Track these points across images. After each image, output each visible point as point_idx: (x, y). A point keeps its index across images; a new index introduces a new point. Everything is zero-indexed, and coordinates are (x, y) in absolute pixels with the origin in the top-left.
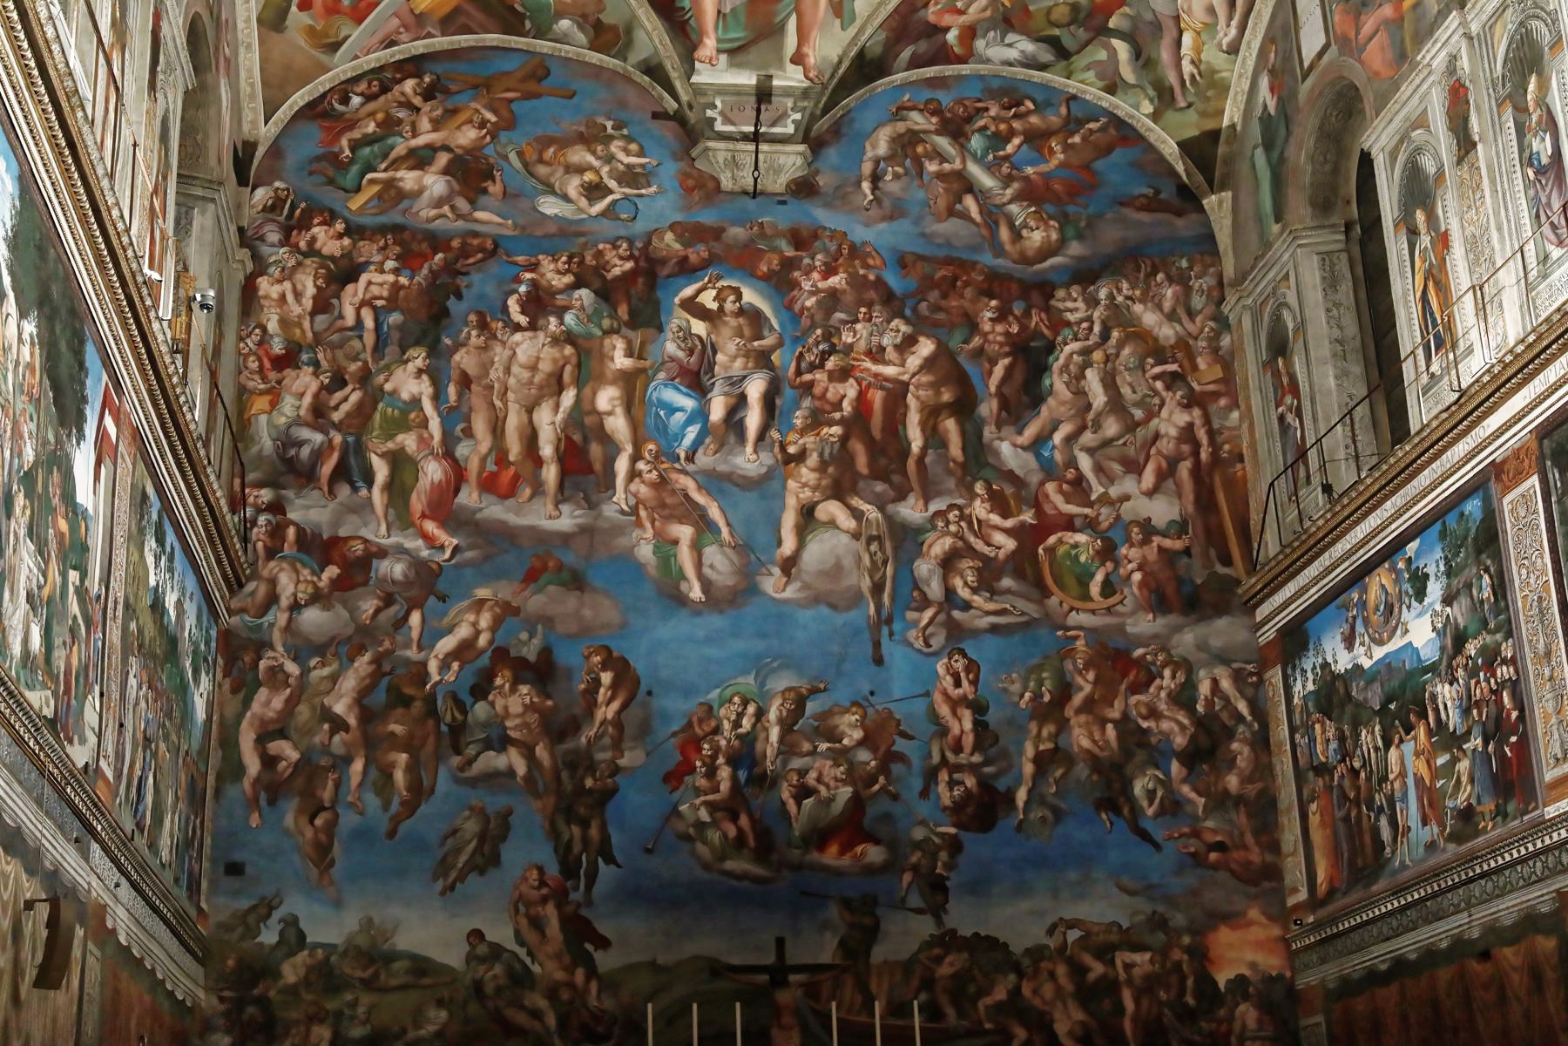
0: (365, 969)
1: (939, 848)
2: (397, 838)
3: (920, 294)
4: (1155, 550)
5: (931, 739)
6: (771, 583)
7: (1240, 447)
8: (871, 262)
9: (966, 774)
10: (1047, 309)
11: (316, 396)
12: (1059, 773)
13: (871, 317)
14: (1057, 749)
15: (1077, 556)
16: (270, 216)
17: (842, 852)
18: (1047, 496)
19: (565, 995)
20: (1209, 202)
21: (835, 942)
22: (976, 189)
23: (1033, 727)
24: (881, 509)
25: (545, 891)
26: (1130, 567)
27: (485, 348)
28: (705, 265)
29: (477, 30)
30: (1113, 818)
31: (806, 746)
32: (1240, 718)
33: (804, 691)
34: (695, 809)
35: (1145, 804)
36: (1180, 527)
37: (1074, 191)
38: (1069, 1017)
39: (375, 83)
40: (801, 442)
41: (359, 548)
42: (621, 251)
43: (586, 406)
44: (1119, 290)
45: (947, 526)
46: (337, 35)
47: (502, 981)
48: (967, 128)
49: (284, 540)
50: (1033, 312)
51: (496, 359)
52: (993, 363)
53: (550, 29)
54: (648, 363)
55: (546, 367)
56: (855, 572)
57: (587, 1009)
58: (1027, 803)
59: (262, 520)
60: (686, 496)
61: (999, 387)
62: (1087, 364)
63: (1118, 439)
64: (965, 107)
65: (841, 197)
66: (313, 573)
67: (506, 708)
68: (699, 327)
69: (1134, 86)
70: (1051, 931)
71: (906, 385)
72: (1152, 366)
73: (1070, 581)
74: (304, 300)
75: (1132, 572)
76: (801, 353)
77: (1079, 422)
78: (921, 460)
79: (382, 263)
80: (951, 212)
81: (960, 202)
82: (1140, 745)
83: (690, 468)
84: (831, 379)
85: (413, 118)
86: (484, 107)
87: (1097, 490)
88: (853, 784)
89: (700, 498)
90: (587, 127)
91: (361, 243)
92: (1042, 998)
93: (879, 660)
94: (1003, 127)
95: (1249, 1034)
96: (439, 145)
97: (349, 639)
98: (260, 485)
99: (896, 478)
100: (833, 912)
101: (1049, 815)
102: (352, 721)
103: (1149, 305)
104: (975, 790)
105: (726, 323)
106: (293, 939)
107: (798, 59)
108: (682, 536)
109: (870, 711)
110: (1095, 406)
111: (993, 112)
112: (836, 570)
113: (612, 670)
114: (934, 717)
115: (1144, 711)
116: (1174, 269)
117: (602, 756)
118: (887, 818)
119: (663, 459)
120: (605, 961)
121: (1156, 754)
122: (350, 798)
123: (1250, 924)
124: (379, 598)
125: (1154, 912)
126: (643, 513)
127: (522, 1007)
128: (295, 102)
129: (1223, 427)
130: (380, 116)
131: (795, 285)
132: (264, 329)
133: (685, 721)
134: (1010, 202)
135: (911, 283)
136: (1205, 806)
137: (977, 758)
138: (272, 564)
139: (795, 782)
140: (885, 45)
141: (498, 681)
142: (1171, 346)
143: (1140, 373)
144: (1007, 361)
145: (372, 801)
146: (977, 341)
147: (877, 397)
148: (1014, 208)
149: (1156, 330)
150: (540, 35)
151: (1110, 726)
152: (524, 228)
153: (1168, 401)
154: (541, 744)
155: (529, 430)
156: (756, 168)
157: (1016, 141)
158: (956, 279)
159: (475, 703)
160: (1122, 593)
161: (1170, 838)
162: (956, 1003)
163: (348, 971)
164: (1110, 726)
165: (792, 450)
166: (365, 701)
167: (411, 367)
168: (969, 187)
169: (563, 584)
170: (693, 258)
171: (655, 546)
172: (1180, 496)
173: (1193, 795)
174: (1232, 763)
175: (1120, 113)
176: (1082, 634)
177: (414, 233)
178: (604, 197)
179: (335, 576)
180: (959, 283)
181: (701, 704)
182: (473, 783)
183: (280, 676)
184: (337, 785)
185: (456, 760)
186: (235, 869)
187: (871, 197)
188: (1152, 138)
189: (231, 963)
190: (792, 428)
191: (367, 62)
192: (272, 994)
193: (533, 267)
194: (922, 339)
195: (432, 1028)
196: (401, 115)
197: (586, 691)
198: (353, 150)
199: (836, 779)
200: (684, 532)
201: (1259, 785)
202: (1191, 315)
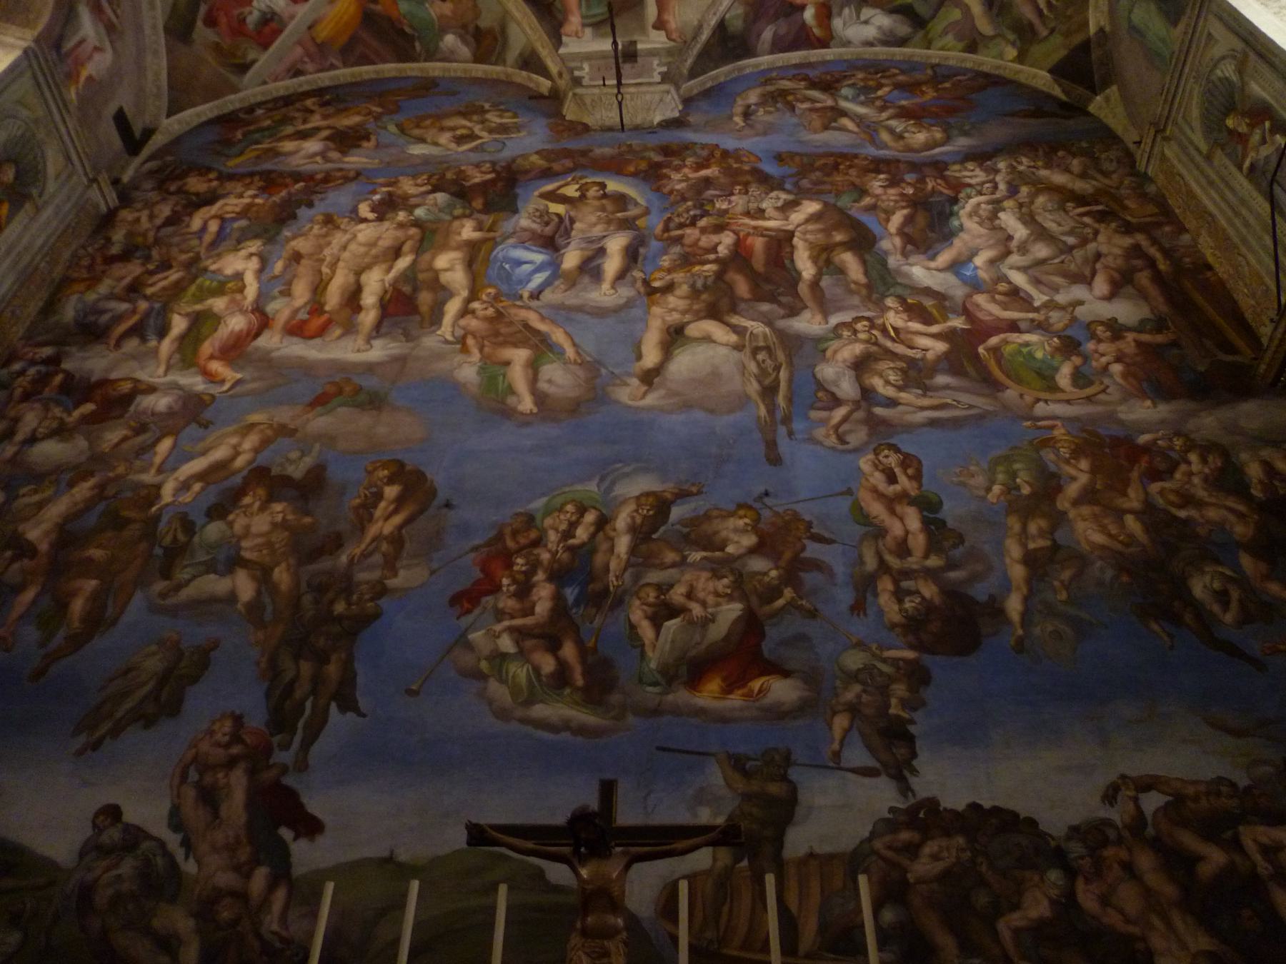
1: (891, 679)
4: (1133, 344)
6: (628, 393)
12: (1066, 575)
14: (1056, 547)
17: (728, 690)
18: (978, 306)
20: (1096, 105)
24: (769, 323)
26: (1104, 360)
28: (570, 170)
33: (668, 496)
35: (1216, 608)
37: (952, 111)
40: (668, 277)
41: (126, 387)
42: (483, 169)
43: (423, 265)
44: (1020, 163)
50: (928, 180)
52: (889, 213)
53: (437, 47)
55: (385, 243)
57: (259, 936)
58: (1025, 615)
64: (832, 76)
67: (247, 527)
69: (992, 38)
70: (1110, 796)
71: (791, 235)
75: (1108, 364)
77: (1002, 248)
78: (815, 285)
83: (534, 303)
87: (1039, 298)
88: (744, 597)
89: (543, 327)
92: (1121, 911)
93: (775, 459)
104: (937, 600)
105: (587, 204)
107: (660, 25)
109: (766, 513)
114: (862, 516)
117: (362, 576)
118: (800, 639)
119: (502, 299)
126: (470, 341)
130: (276, 118)
133: (492, 533)
134: (888, 119)
137: (934, 561)
139: (651, 599)
140: (745, 21)
141: (247, 500)
147: (758, 244)
148: (893, 123)
150: (431, 55)
154: (284, 565)
158: (839, 164)
159: (208, 523)
160: (1102, 383)
165: (656, 284)
167: (243, 253)
168: (844, 113)
169: (357, 406)
176: (1058, 423)
177: (281, 174)
181: (517, 514)
182: (174, 612)
185: (160, 586)
190: (660, 269)
197: (363, 506)
199: (717, 594)
200: (520, 355)
202: (1106, 174)
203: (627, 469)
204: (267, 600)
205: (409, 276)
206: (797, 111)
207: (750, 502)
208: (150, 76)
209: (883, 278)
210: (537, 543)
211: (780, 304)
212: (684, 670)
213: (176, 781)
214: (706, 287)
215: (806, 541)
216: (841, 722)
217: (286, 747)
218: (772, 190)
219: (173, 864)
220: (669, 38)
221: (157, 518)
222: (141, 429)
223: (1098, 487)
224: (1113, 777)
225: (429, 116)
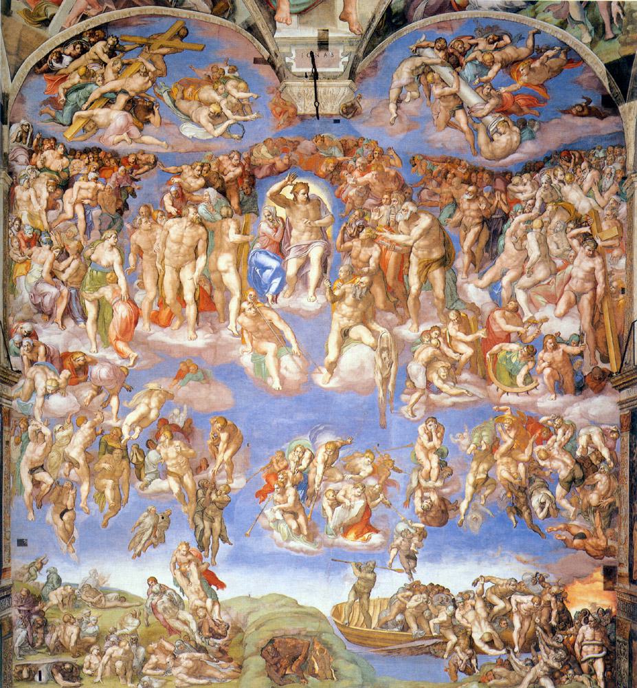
2: (108, 527)
3: (424, 183)
4: (561, 354)
8: (392, 162)
9: (432, 493)
10: (506, 191)
11: (52, 264)
12: (487, 492)
13: (390, 202)
14: (487, 477)
15: (510, 358)
16: (20, 144)
17: (357, 537)
18: (495, 320)
19: (201, 613)
22: (465, 106)
23: (474, 465)
24: (390, 330)
25: (190, 557)
26: (544, 365)
27: (150, 230)
29: (139, 4)
31: (339, 477)
32: (603, 460)
33: (338, 444)
35: (538, 510)
36: (579, 338)
38: (482, 630)
40: (342, 287)
41: (80, 360)
42: (233, 161)
43: (212, 267)
44: (555, 176)
47: (167, 605)
48: (462, 60)
51: (158, 237)
52: (467, 229)
54: (249, 238)
55: (187, 241)
56: (372, 369)
58: (467, 510)
59: (25, 342)
61: (470, 248)
63: (544, 280)
67: (167, 454)
68: (282, 212)
70: (475, 584)
72: (572, 229)
73: (505, 375)
74: (42, 201)
78: (417, 297)
80: (448, 124)
81: (454, 116)
83: (275, 306)
84: (362, 245)
85: (102, 71)
86: (146, 60)
87: (527, 315)
89: (280, 325)
91: (74, 161)
93: (384, 427)
94: (487, 57)
95: (585, 642)
96: (119, 89)
98: (24, 321)
100: (351, 570)
102: (81, 461)
105: (298, 209)
112: (362, 368)
115: (543, 455)
116: (594, 159)
117: (221, 482)
120: (222, 595)
122: (81, 505)
125: (537, 573)
126: (246, 336)
127: (178, 619)
130: (82, 70)
131: (341, 181)
137: (439, 484)
138: (32, 369)
139: (331, 497)
141: (162, 438)
143: (563, 234)
144: (477, 229)
146: (458, 216)
147: (392, 257)
148: (490, 119)
149: (576, 206)
153: (579, 254)
155: (178, 283)
157: (496, 68)
159: (149, 451)
162: (416, 619)
163: (84, 598)
165: (337, 293)
167: (107, 244)
169: (198, 380)
170: (279, 165)
173: (568, 506)
174: (594, 486)
175: (568, 42)
178: (223, 122)
180: (449, 176)
183: (40, 435)
185: (139, 484)
187: (395, 115)
192: (45, 609)
193: (179, 174)
194: (422, 216)
196: (95, 69)
197: (213, 444)
198: (66, 96)
199: (355, 496)
200: (270, 347)
201: (610, 500)
202: (601, 191)
203: (321, 428)
205: (205, 277)
210: (286, 467)
211: (397, 314)
216: (394, 552)
218: (405, 201)
222: (99, 390)
225: (189, 83)
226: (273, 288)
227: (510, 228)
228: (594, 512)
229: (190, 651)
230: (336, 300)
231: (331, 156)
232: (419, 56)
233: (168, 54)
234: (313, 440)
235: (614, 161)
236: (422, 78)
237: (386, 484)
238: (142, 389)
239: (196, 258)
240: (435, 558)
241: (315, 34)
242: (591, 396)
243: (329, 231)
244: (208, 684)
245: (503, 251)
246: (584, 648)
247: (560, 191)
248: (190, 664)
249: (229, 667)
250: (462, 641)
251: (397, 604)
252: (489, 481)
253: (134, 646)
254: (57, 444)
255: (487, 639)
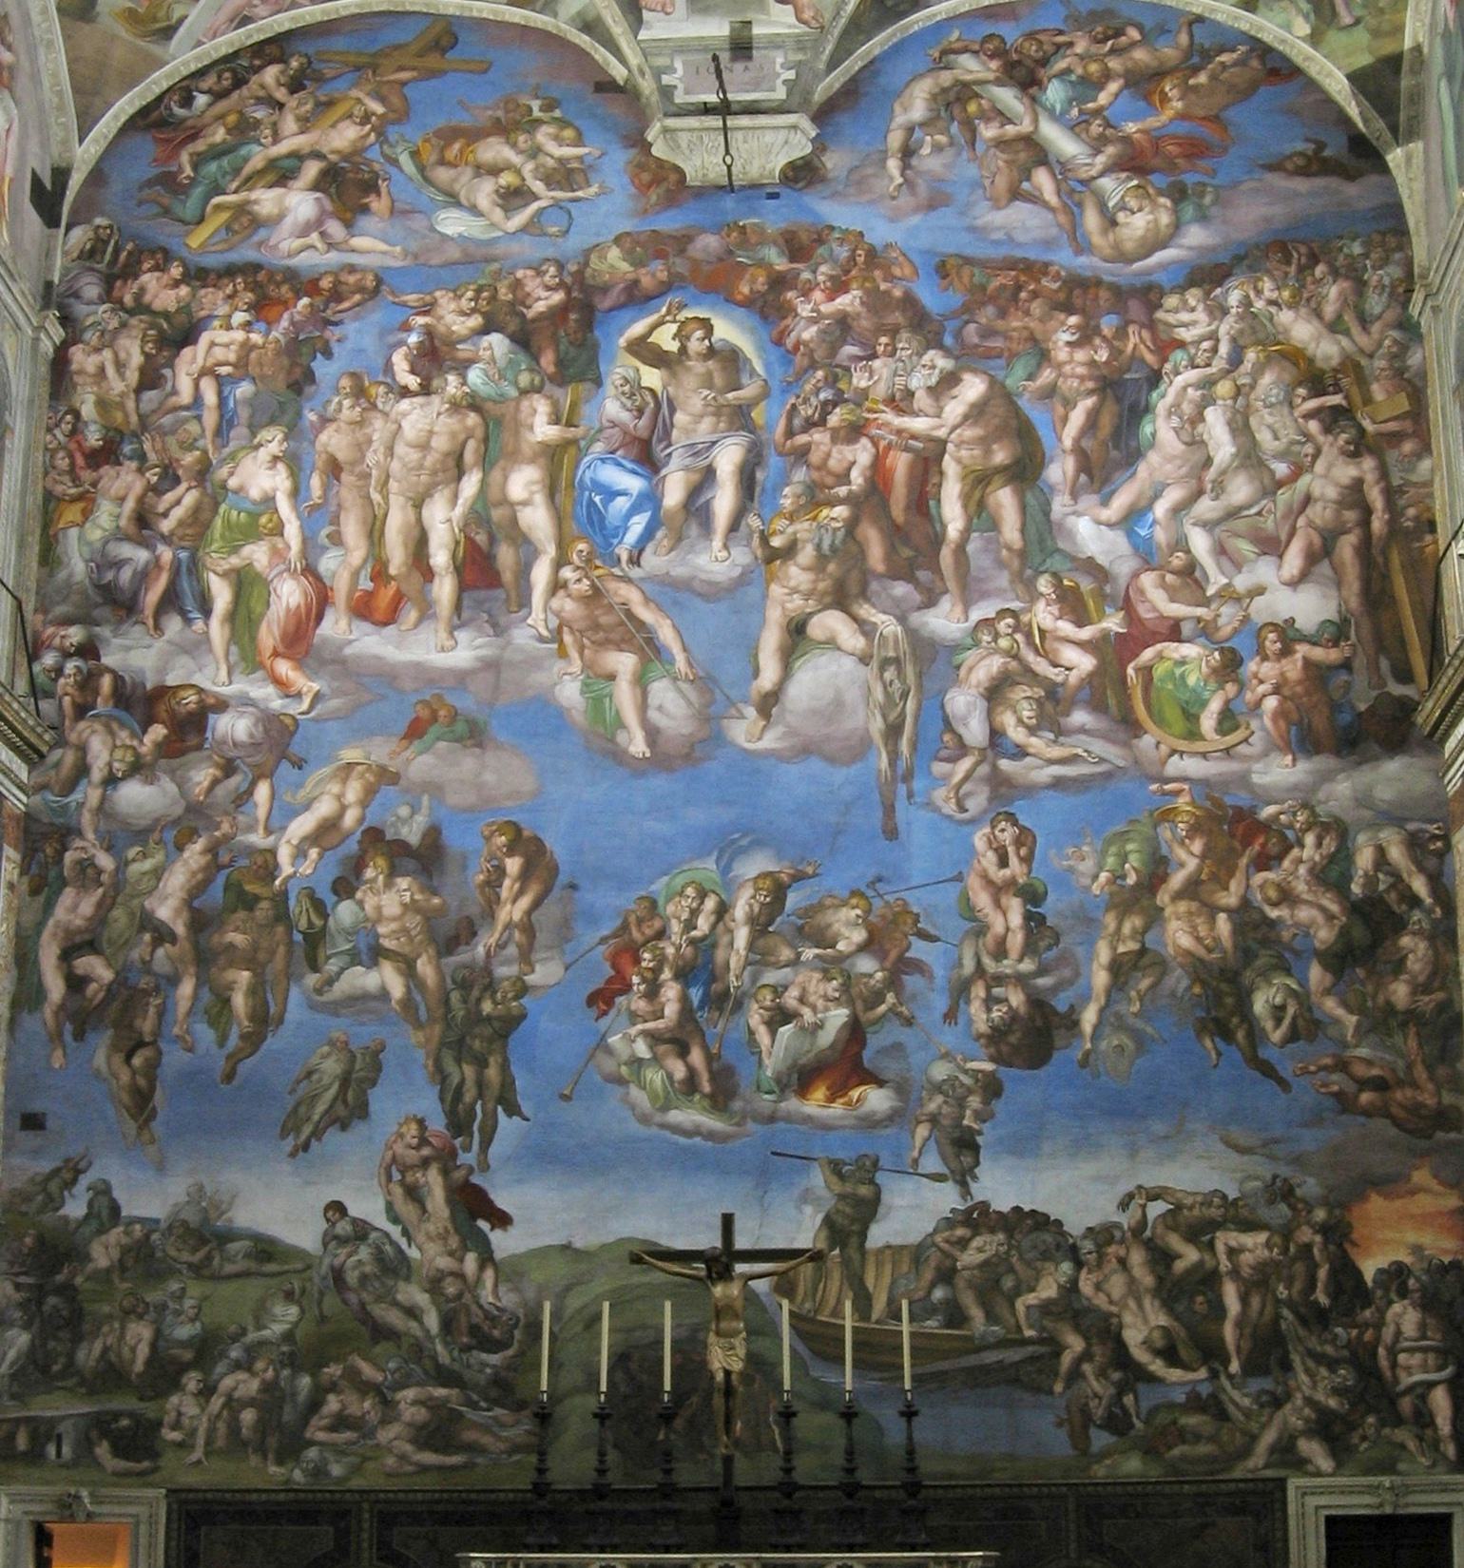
0: (194, 1250)
3: (968, 310)
4: (1300, 664)
5: (962, 942)
6: (744, 730)
7: (1430, 509)
8: (897, 272)
9: (1011, 989)
10: (1151, 325)
11: (141, 500)
12: (1145, 984)
13: (895, 350)
14: (1143, 951)
15: (1183, 677)
17: (831, 1099)
18: (1142, 592)
20: (1395, 157)
21: (820, 1217)
22: (1052, 158)
24: (902, 620)
25: (426, 1151)
26: (1262, 689)
27: (361, 423)
28: (665, 288)
30: (1221, 1045)
31: (786, 954)
32: (1415, 901)
33: (784, 878)
34: (628, 1041)
35: (1269, 1025)
36: (1337, 631)
37: (1195, 150)
38: (1146, 1321)
39: (227, 75)
40: (790, 530)
41: (191, 699)
42: (547, 278)
43: (494, 493)
44: (1259, 292)
45: (995, 640)
46: (168, 19)
47: (368, 1269)
48: (1042, 73)
49: (96, 692)
50: (1131, 329)
52: (1069, 404)
55: (441, 444)
57: (481, 1307)
58: (1096, 1028)
59: (70, 667)
60: (629, 614)
61: (1077, 441)
62: (1207, 401)
63: (1249, 506)
64: (1040, 42)
65: (857, 182)
66: (133, 735)
67: (379, 908)
68: (652, 377)
70: (1124, 1205)
71: (941, 445)
72: (1304, 399)
73: (1172, 714)
74: (128, 373)
76: (794, 406)
78: (960, 549)
79: (230, 316)
80: (1015, 194)
81: (1028, 179)
82: (1265, 942)
83: (635, 573)
84: (834, 440)
87: (1216, 581)
88: (851, 1003)
90: (507, 112)
91: (203, 292)
92: (1109, 1296)
93: (891, 833)
94: (1093, 68)
96: (307, 150)
97: (176, 822)
98: (68, 621)
99: (923, 575)
100: (817, 1178)
101: (1129, 1044)
102: (180, 929)
103: (1303, 311)
104: (1022, 1010)
105: (689, 369)
106: (105, 1213)
108: (621, 668)
109: (877, 903)
110: (1216, 461)
111: (1079, 49)
112: (838, 703)
113: (521, 855)
114: (969, 911)
115: (1273, 894)
117: (504, 971)
119: (598, 563)
120: (504, 1243)
121: (1287, 955)
122: (176, 1030)
123: (1413, 1193)
124: (217, 765)
125: (1275, 1177)
126: (568, 638)
127: (396, 1304)
128: (122, 109)
129: (1408, 483)
130: (232, 119)
131: (788, 310)
132: (77, 415)
133: (618, 922)
134: (1102, 174)
135: (955, 298)
136: (1358, 1027)
137: (1027, 966)
138: (82, 725)
141: (369, 873)
142: (1335, 370)
143: (1286, 410)
144: (1089, 402)
145: (205, 1034)
146: (1047, 375)
147: (900, 464)
148: (1107, 183)
149: (1311, 349)
151: (1222, 917)
152: (416, 257)
153: (1325, 449)
155: (416, 532)
156: (727, 152)
157: (1113, 87)
158: (1019, 288)
159: (337, 903)
160: (1248, 727)
161: (1305, 1072)
163: (173, 1253)
164: (1222, 917)
165: (776, 542)
166: (196, 904)
167: (263, 454)
169: (457, 741)
170: (646, 282)
171: (585, 685)
172: (1339, 584)
173: (1340, 1012)
174: (1399, 966)
176: (1186, 787)
177: (271, 275)
178: (526, 205)
179: (160, 738)
180: (1023, 295)
183: (90, 871)
184: (161, 1014)
185: (312, 979)
186: (32, 1122)
187: (900, 180)
188: (1313, 71)
189: (28, 1240)
191: (216, 49)
192: (79, 1280)
193: (427, 309)
194: (967, 377)
195: (276, 1329)
197: (487, 883)
198: (195, 167)
199: (826, 998)
200: (624, 663)
201: (1440, 996)
202: (1364, 322)
203: (744, 842)
204: (419, 998)
205: (478, 516)
206: (980, 147)
207: (863, 889)
208: (46, 83)
209: (1041, 541)
212: (795, 1076)
213: (383, 1179)
214: (833, 549)
215: (911, 938)
216: (922, 1131)
217: (467, 1149)
218: (928, 347)
219: (401, 1251)
220: (800, 20)
221: (284, 894)
222: (229, 769)
223: (1203, 877)
224: (1130, 1187)
226: (632, 536)
227: (1164, 399)
228: (1403, 1025)
229: (419, 1384)
230: (776, 557)
231: (761, 264)
232: (946, 68)
233: (414, 80)
234: (725, 870)
235: (1384, 262)
236: (956, 110)
237: (902, 968)
238: (330, 759)
239: (459, 478)
240: (1024, 1146)
241: (724, 30)
242: (1377, 758)
243: (757, 415)
244: (465, 1466)
245: (1152, 445)
246: (1402, 1358)
247: (1271, 319)
248: (421, 1414)
249: (517, 1423)
250: (1097, 1350)
251: (934, 1258)
252: (1145, 961)
253: (286, 1372)
254: (128, 890)
255: (1159, 1343)
